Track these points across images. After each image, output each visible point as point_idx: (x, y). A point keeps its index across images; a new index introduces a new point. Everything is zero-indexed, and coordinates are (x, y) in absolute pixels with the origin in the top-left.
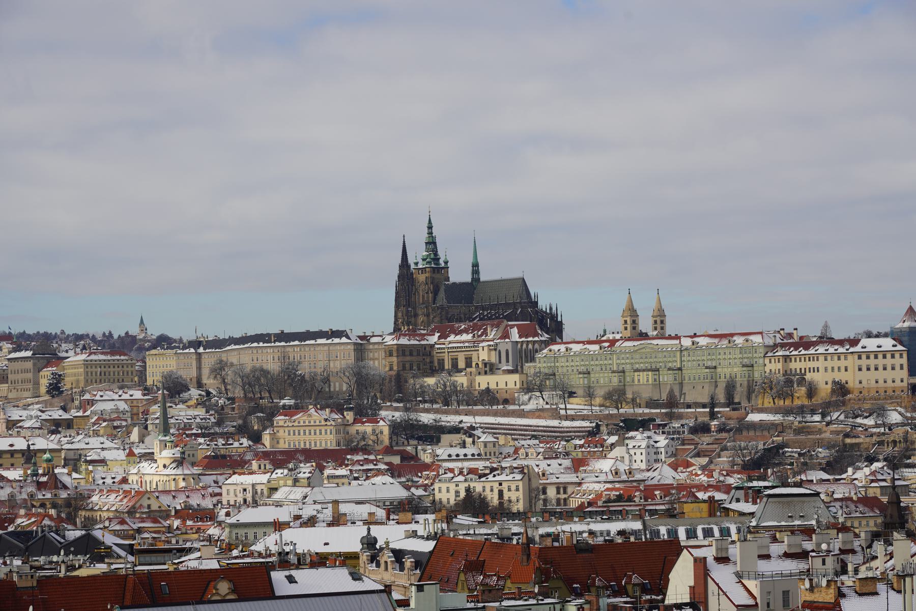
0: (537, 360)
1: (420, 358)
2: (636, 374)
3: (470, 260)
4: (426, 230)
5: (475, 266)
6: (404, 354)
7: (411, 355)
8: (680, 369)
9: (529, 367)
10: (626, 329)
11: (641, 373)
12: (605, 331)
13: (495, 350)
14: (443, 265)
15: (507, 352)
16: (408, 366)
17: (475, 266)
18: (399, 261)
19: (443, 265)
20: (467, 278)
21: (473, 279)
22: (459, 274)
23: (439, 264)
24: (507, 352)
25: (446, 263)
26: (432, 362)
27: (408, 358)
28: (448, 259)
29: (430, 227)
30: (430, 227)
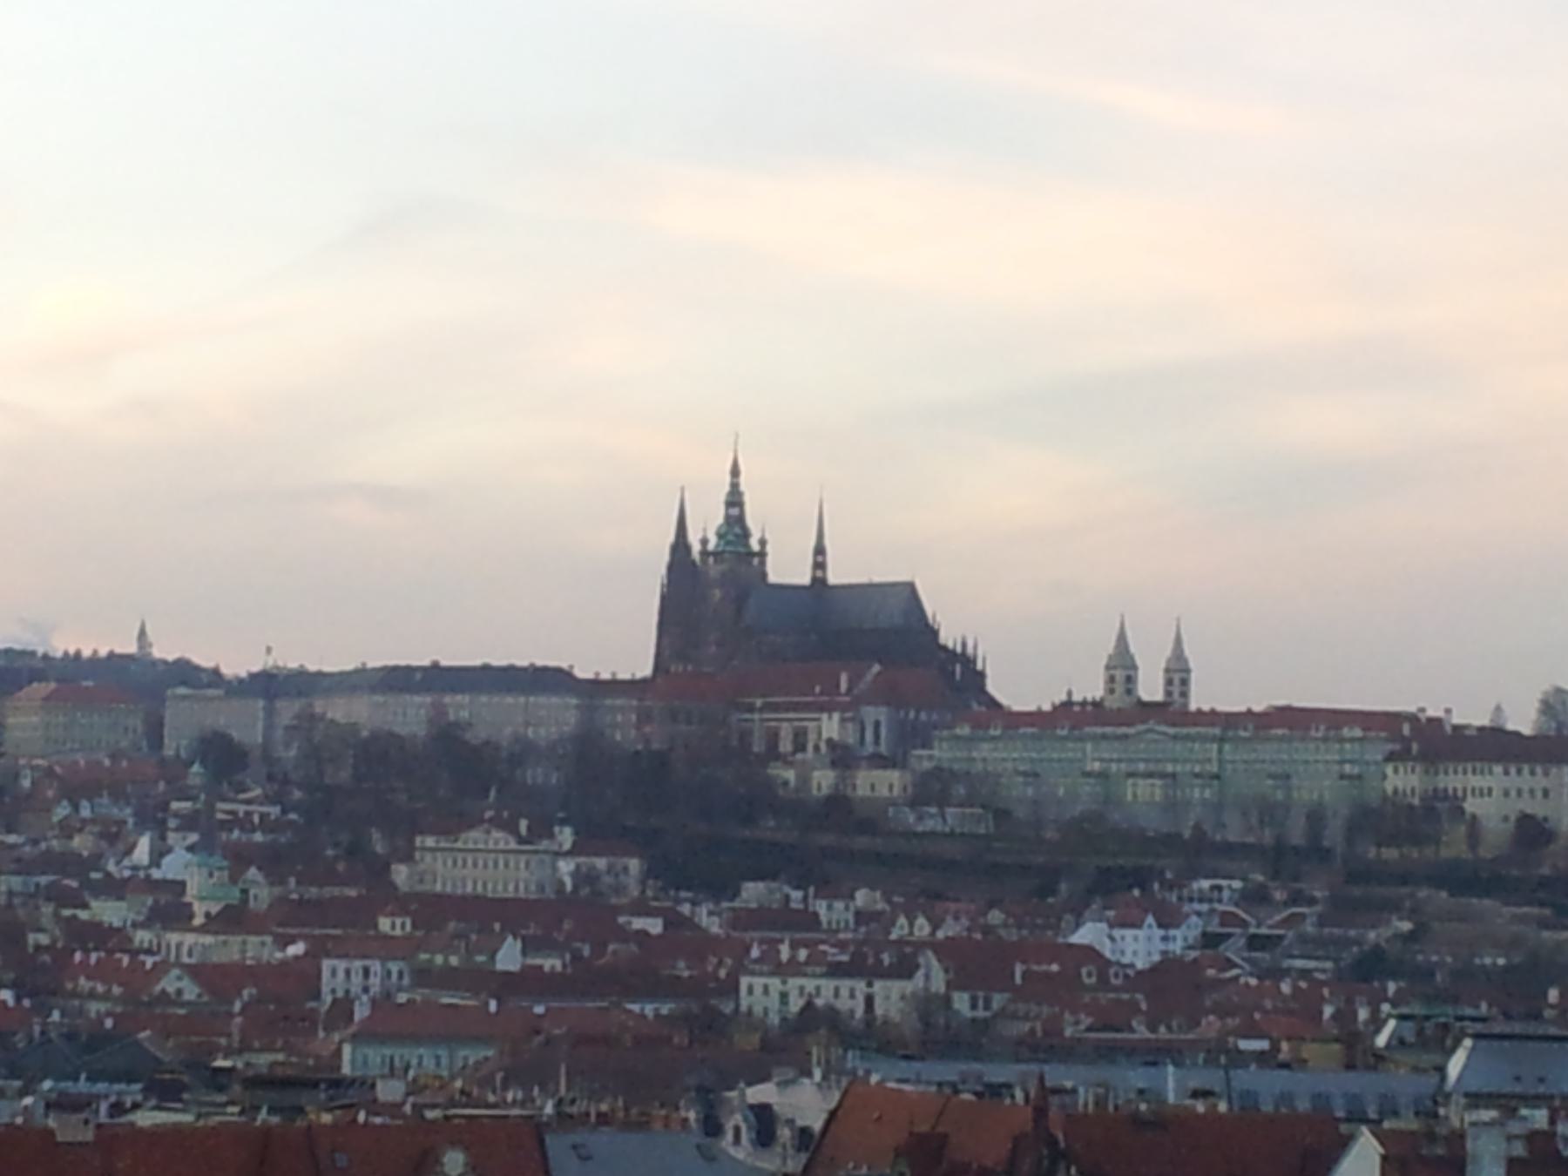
0: (936, 744)
2: (1130, 781)
3: (812, 543)
4: (728, 479)
5: (820, 550)
7: (689, 722)
8: (1217, 777)
9: (920, 757)
10: (1112, 691)
11: (1141, 782)
12: (1070, 693)
13: (852, 719)
14: (755, 546)
15: (877, 725)
18: (671, 537)
20: (802, 576)
21: (814, 579)
23: (747, 545)
24: (877, 725)
25: (763, 542)
28: (768, 537)
29: (735, 472)
30: (735, 472)
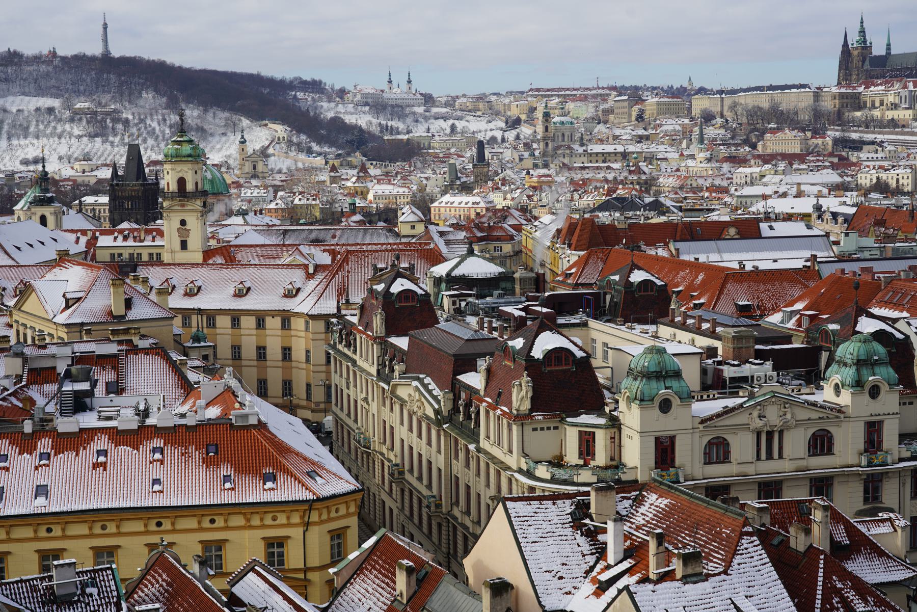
1: (853, 101)
3: (886, 42)
4: (859, 24)
5: (889, 45)
6: (843, 98)
7: (847, 98)
14: (869, 45)
16: (845, 105)
17: (889, 45)
19: (869, 45)
20: (883, 53)
22: (878, 50)
25: (871, 43)
26: (859, 103)
27: (846, 100)
29: (862, 22)
30: (862, 22)
